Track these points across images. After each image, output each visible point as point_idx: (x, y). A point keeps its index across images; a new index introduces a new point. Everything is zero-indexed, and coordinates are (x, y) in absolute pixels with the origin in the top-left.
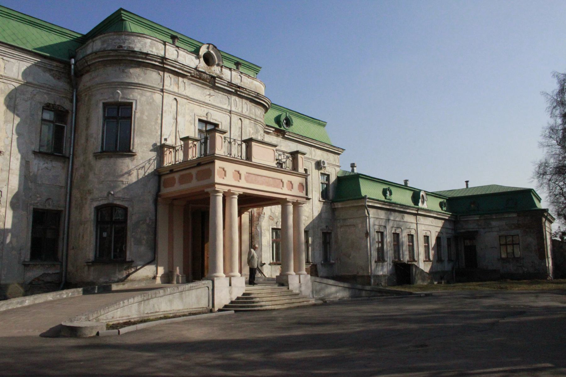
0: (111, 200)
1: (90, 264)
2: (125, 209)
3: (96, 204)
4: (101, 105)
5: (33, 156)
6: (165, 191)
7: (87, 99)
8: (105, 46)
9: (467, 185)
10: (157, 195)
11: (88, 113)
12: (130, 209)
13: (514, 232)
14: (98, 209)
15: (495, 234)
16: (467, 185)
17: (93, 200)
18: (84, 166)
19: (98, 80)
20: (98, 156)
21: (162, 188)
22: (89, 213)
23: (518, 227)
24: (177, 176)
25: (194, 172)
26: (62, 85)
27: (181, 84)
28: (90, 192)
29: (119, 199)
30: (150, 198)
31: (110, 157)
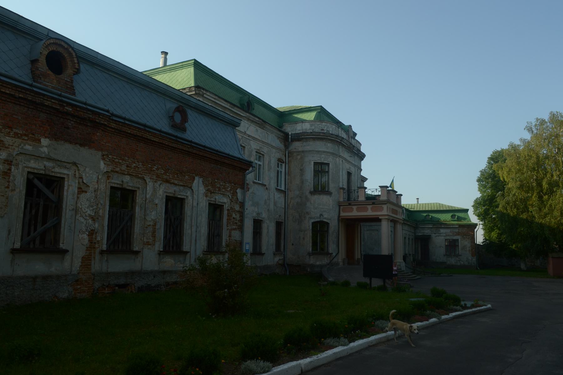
0: (322, 219)
1: (309, 254)
2: (328, 224)
3: (313, 221)
4: (313, 163)
5: (275, 190)
6: (343, 214)
7: (299, 157)
8: (313, 127)
9: (418, 201)
10: (339, 216)
11: (302, 166)
12: (330, 224)
13: (455, 238)
14: (313, 223)
15: (443, 237)
16: (418, 201)
17: (311, 218)
18: (300, 197)
19: (308, 148)
20: (311, 193)
21: (341, 212)
22: (308, 225)
23: (458, 234)
24: (355, 207)
25: (369, 207)
26: (282, 146)
27: (341, 150)
28: (308, 213)
29: (325, 218)
30: (336, 217)
31: (320, 194)
